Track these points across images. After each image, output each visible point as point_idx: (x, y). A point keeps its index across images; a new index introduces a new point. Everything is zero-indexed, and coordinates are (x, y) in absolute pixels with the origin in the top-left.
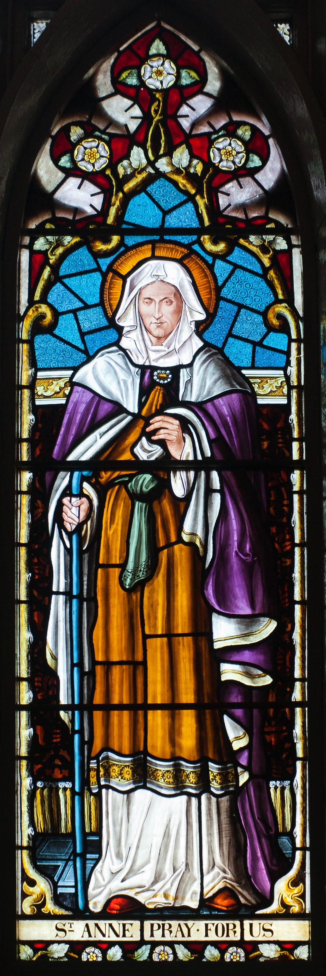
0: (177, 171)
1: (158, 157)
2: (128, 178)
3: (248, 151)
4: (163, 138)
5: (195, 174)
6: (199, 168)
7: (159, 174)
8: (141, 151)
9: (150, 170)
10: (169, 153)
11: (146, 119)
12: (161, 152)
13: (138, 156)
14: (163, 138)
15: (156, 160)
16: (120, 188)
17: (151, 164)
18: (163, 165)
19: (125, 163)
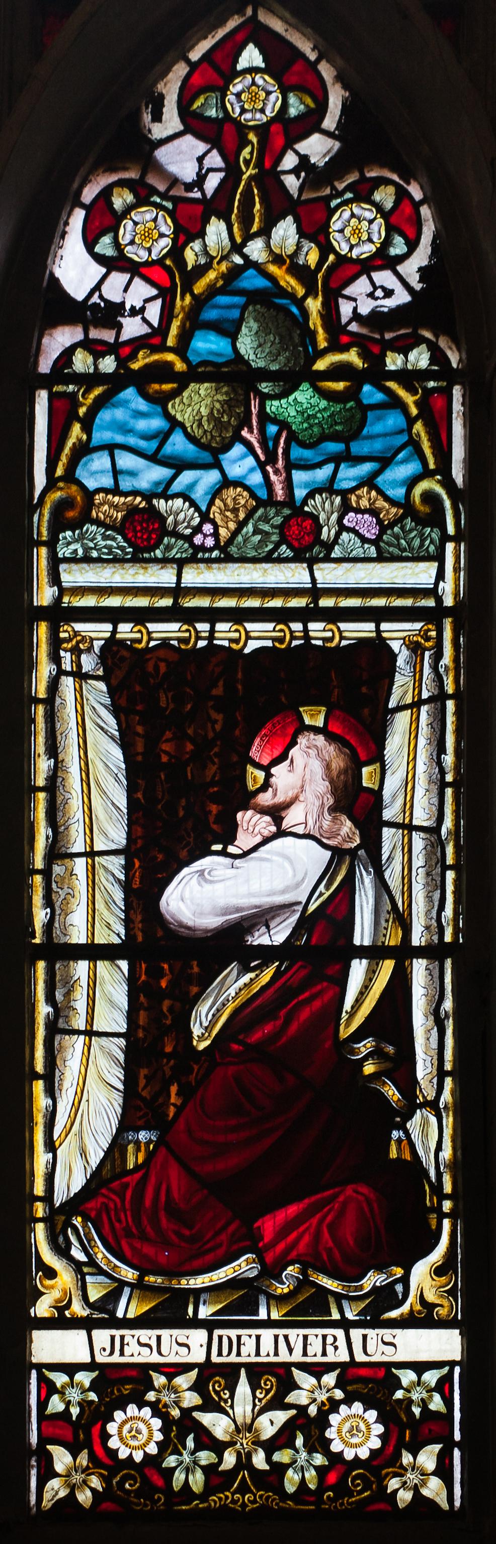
0: (278, 259)
1: (248, 237)
2: (201, 270)
3: (391, 229)
4: (258, 206)
5: (306, 267)
6: (312, 257)
7: (249, 263)
8: (222, 226)
9: (238, 260)
10: (266, 232)
11: (232, 172)
12: (255, 228)
13: (216, 233)
14: (258, 206)
15: (244, 244)
16: (187, 288)
17: (237, 248)
18: (256, 250)
19: (197, 245)
